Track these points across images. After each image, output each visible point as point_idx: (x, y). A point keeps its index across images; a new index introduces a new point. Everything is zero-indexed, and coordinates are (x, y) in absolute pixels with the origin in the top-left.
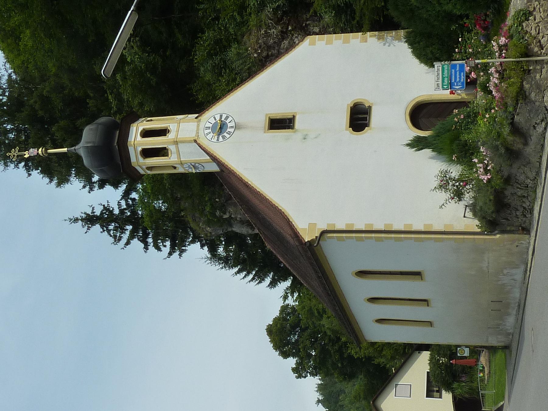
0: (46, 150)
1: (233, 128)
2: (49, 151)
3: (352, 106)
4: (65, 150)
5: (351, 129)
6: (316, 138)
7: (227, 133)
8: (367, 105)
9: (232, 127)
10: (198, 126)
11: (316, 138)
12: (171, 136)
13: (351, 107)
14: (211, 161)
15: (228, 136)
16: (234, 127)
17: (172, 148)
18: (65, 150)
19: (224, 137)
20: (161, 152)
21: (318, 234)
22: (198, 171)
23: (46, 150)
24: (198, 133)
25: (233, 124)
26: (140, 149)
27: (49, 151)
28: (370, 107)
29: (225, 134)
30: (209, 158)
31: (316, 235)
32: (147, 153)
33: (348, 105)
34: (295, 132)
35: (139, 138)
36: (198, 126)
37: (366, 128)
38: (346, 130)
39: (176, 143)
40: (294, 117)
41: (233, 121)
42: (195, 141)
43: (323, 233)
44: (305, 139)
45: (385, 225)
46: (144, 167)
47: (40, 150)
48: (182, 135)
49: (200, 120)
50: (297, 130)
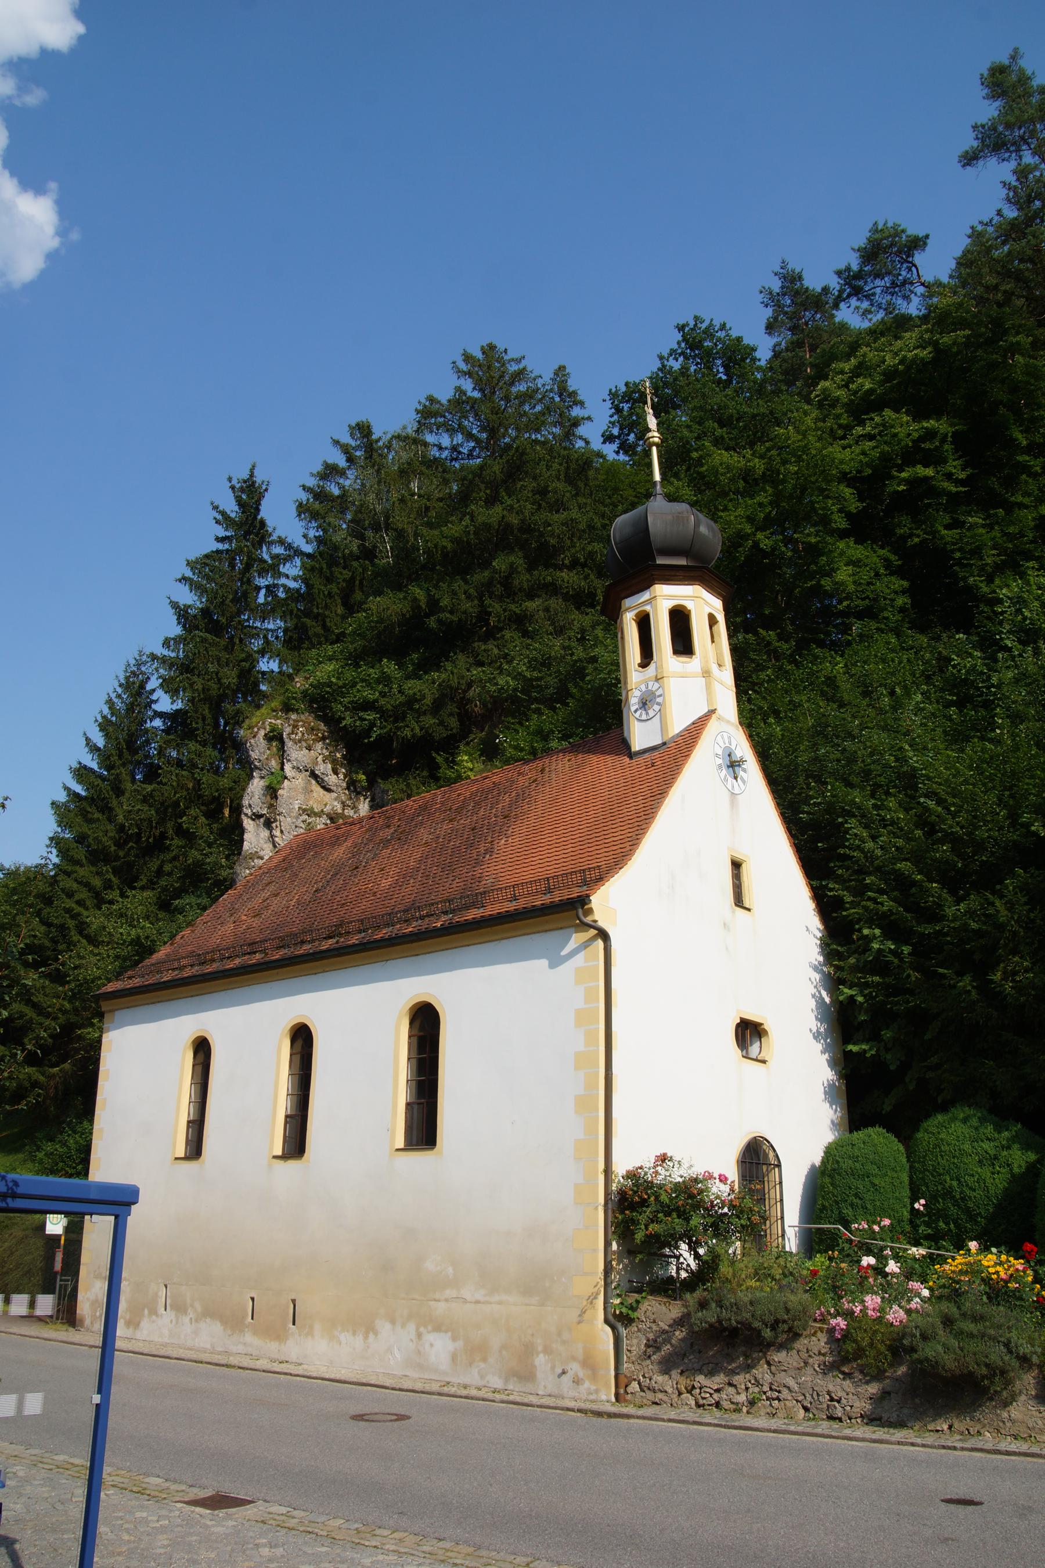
0: (657, 445)
2: (654, 449)
4: (657, 477)
6: (727, 949)
10: (733, 724)
13: (762, 1024)
14: (670, 735)
17: (693, 664)
18: (657, 477)
19: (720, 766)
20: (683, 644)
21: (601, 924)
22: (633, 709)
23: (657, 445)
26: (689, 605)
27: (654, 449)
30: (677, 731)
32: (680, 619)
35: (709, 610)
36: (733, 724)
39: (706, 674)
40: (749, 910)
43: (604, 935)
46: (648, 608)
47: (656, 434)
48: (717, 687)
50: (734, 912)
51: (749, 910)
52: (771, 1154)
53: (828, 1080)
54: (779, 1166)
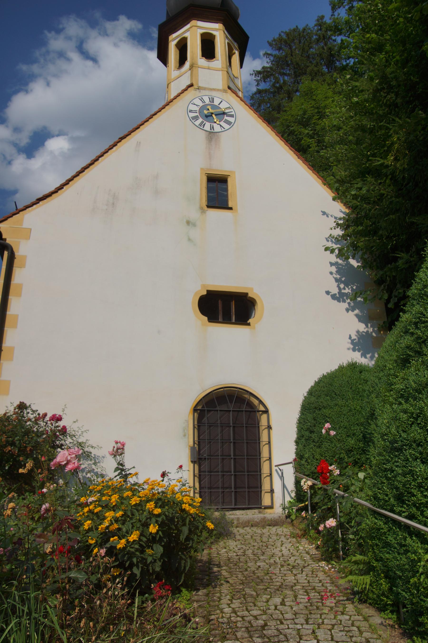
1: (211, 129)
3: (250, 295)
5: (205, 293)
6: (189, 240)
7: (203, 122)
8: (250, 321)
9: (212, 128)
11: (189, 240)
12: (202, 62)
13: (247, 294)
15: (198, 123)
16: (213, 131)
19: (196, 118)
24: (205, 89)
25: (217, 128)
26: (187, 35)
28: (249, 324)
29: (200, 120)
31: (7, 239)
33: (252, 289)
34: (201, 208)
37: (206, 318)
38: (203, 286)
40: (231, 209)
41: (223, 130)
42: (191, 85)
44: (188, 223)
45: (12, 349)
49: (224, 91)
50: (203, 211)
51: (231, 209)
52: (256, 402)
53: (358, 332)
54: (266, 412)
